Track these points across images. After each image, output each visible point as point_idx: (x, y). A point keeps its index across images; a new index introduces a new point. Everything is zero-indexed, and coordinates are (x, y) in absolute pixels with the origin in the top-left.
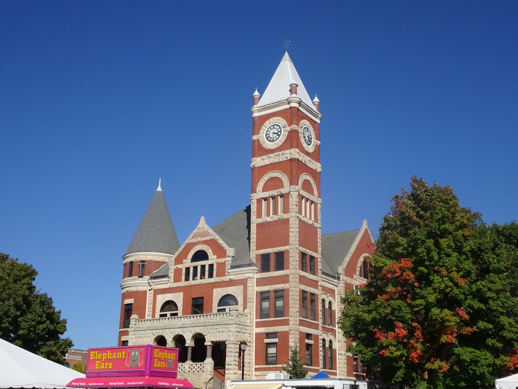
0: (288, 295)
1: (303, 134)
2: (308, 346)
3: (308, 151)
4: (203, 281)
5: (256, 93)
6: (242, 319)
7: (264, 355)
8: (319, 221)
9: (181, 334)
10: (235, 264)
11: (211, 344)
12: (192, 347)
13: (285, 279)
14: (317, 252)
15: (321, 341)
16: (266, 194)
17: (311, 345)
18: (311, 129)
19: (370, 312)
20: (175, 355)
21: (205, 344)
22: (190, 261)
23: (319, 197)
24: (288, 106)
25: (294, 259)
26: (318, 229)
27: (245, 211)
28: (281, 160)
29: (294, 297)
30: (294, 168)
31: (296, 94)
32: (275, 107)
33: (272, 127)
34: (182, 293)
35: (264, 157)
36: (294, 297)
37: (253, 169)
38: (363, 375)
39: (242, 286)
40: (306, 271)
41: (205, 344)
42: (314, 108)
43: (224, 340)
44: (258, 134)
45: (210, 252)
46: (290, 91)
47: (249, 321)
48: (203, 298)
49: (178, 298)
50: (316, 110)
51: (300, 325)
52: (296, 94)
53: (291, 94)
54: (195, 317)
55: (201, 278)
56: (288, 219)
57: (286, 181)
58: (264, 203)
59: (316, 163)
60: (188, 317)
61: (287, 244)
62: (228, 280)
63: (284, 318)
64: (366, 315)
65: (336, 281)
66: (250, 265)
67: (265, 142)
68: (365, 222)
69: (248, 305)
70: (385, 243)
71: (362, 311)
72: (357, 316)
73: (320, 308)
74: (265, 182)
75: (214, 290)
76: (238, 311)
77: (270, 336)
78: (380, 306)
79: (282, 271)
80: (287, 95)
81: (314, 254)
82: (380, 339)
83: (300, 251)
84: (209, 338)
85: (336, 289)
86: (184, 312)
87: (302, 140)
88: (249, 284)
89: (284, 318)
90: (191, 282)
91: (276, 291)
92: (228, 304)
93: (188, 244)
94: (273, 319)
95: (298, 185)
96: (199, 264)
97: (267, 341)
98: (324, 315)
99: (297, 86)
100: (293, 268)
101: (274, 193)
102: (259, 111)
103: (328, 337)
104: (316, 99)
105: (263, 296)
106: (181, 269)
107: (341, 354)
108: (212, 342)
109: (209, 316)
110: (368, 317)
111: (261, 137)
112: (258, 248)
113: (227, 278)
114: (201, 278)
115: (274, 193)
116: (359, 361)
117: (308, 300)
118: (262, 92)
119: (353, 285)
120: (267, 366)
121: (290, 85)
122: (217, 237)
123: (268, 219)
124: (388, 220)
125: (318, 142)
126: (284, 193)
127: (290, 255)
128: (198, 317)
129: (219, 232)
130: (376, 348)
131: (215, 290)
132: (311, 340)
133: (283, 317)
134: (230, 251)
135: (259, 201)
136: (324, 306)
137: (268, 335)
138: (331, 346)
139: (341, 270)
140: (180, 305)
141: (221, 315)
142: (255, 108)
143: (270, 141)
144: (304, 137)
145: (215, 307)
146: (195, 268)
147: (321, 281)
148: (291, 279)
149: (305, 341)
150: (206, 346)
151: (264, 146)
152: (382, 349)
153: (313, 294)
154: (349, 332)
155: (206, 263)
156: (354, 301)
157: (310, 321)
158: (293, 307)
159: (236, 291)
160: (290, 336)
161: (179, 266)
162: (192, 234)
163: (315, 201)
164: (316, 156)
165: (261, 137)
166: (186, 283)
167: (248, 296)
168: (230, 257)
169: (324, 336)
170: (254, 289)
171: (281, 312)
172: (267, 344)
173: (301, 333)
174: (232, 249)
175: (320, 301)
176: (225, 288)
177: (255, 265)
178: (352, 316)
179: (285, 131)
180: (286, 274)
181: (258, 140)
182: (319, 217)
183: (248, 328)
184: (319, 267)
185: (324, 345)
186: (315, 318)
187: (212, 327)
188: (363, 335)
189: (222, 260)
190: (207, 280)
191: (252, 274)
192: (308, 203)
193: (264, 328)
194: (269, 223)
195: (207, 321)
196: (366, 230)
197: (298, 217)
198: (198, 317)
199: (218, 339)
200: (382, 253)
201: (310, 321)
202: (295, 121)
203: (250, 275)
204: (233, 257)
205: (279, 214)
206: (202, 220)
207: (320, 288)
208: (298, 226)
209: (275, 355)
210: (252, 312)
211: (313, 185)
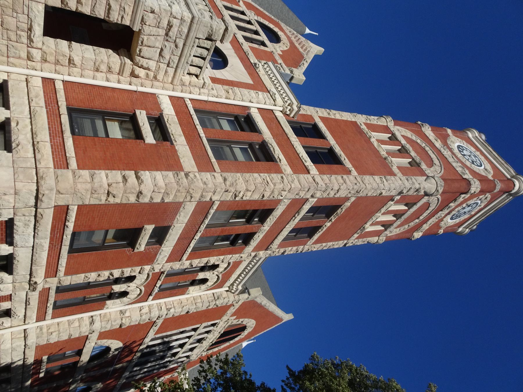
17: (132, 244)
24: (509, 177)
38: (40, 373)
62: (252, 62)
63: (213, 160)
65: (240, 288)
91: (264, 147)
94: (202, 135)
97: (142, 117)
107: (92, 322)
116: (76, 359)
120: (63, 110)
127: (345, 177)
138: (112, 296)
149: (149, 224)
160: (170, 174)
168: (292, 72)
169: (140, 279)
172: (133, 119)
183: (171, 71)
193: (173, 113)
210: (205, 91)
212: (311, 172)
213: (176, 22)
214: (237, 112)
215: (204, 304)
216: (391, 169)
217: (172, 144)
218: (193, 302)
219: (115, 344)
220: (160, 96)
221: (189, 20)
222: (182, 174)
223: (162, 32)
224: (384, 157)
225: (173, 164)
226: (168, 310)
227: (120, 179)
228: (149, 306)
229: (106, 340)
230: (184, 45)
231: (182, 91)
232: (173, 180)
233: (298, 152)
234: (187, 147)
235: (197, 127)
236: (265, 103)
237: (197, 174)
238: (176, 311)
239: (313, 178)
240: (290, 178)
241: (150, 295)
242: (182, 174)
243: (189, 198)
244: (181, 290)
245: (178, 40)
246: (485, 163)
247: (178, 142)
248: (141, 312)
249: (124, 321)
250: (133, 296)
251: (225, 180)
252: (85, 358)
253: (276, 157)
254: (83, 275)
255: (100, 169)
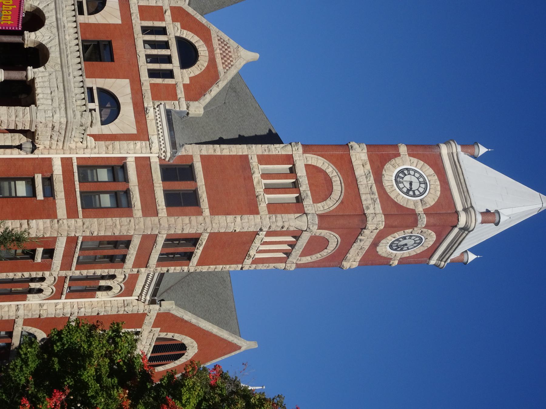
0: (121, 216)
1: (411, 236)
2: (32, 254)
3: (381, 244)
4: (142, 60)
5: (482, 150)
6: (76, 134)
7: (11, 174)
8: (254, 266)
9: (47, 22)
10: (175, 117)
11: (30, 77)
12: (23, 44)
13: (150, 210)
14: (200, 263)
15: (40, 275)
16: (301, 172)
18: (419, 250)
19: (98, 379)
20: (9, 22)
21: (29, 68)
22: (178, 34)
23: (298, 266)
24: (459, 207)
25: (185, 224)
26: (240, 266)
27: (270, 130)
28: (363, 197)
29: (118, 227)
30: (349, 220)
31: (482, 223)
32: (458, 185)
33: (421, 180)
34: (120, 22)
35: (368, 167)
36: (118, 227)
37: (347, 147)
39: (135, 132)
40: (165, 246)
41: (29, 68)
42: (456, 254)
43: (38, 103)
44: (410, 155)
45: (195, 70)
46: (488, 211)
47: (73, 145)
48: (112, 60)
49: (111, 15)
50: (452, 257)
51: (68, 238)
52: (482, 223)
53: (482, 213)
54: (77, 48)
55: (147, 56)
56: (257, 213)
57: (326, 207)
58: (285, 168)
59: (359, 258)
60: (76, 35)
61: (214, 211)
62: (146, 105)
63: (80, 209)
64: (92, 371)
65: (148, 298)
66: (174, 145)
67: (395, 167)
68: (253, 345)
69: (103, 143)
70: (222, 401)
71: (99, 365)
72: (90, 355)
73: (99, 272)
74: (324, 168)
75: (127, 81)
76: (91, 126)
77: (47, 183)
78: (110, 396)
79: (164, 203)
80: (480, 206)
81: (195, 260)
82: (51, 398)
83: (201, 234)
84: (40, 75)
85: (134, 298)
86: (85, 27)
87: (398, 235)
88: (139, 143)
89: (80, 209)
90: (140, 38)
91: (127, 192)
92: (102, 106)
93: (208, 31)
94: (78, 190)
95: (319, 228)
96: (174, 52)
97: (38, 179)
98: (87, 278)
99: (497, 224)
100: (170, 224)
101: (305, 187)
102: (451, 155)
103: (47, 286)
104: (472, 257)
105: (118, 169)
106: (162, 19)
107: (17, 310)
108: (33, 80)
109: (80, 73)
110: (88, 374)
111: (405, 160)
112: (203, 157)
113: (148, 103)
114: (147, 56)
115: (305, 187)
116: (8, 340)
117: (112, 250)
118: (483, 159)
119: (141, 327)
121: (497, 212)
122: (222, 84)
123: (257, 177)
124: (262, 405)
125: (396, 263)
126: (305, 203)
127: (193, 218)
128: (78, 54)
129: (231, 87)
130: (31, 389)
131: (127, 82)
132: (43, 258)
133: (82, 208)
134: (197, 109)
135: (289, 159)
136: (103, 278)
137: (48, 181)
138: (31, 291)
139: (168, 306)
140: (98, 19)
141: (83, 96)
142: (456, 148)
143: (397, 176)
144: (404, 238)
145: (96, 83)
146: (165, 45)
147: (147, 272)
148: (151, 220)
149: (40, 247)
150: (26, 70)
151: (388, 166)
152: (31, 402)
153: (123, 259)
154: (61, 339)
155: (175, 65)
156: (116, 347)
157: (76, 255)
158: (99, 224)
159: (126, 121)
160: (48, 221)
161: (168, 16)
162: (226, 38)
163: (291, 259)
164: (371, 258)
165: (405, 160)
166: (137, 29)
167: (117, 143)
168: (188, 108)
169: (49, 280)
170: (130, 152)
171: (90, 203)
173: (54, 239)
174: (201, 112)
175: (112, 272)
176: (131, 101)
177: (173, 155)
178: (90, 345)
179: (415, 203)
180: (160, 211)
181: (399, 155)
182: (261, 267)
183: (60, 144)
184: (173, 268)
185: (33, 280)
186: (81, 264)
187: (60, 79)
188: (57, 366)
189: (181, 94)
190: (144, 67)
191: (157, 149)
192: (286, 247)
193: (61, 172)
194: (250, 178)
195: (71, 70)
196: (240, 348)
197: (261, 230)
198: (78, 54)
199: (38, 91)
200: (204, 397)
201: (76, 255)
202: (432, 221)
203: (155, 146)
204: (188, 114)
205: (267, 196)
206: (253, 56)
207: (135, 270)
208: (245, 230)
209: (14, 195)
210: (89, 150)
211: (318, 255)
212: (159, 215)
213: (55, 125)
214: (113, 164)
215: (113, 309)
216: (258, 207)
217: (54, 199)
218: (103, 305)
219: (41, 335)
220: (54, 159)
221: (65, 123)
222: (56, 220)
223: (49, 129)
224: (257, 194)
225: (52, 214)
226: (79, 309)
227: (18, 225)
228: (64, 304)
229: (30, 328)
230: (65, 132)
231: (70, 153)
232: (49, 225)
233: (156, 197)
234: (64, 201)
235: (76, 183)
236: (141, 153)
237: (65, 221)
238: (87, 311)
239: (159, 220)
240: (137, 221)
241: (62, 294)
242: (56, 220)
243: (60, 235)
244: (89, 293)
245: (60, 131)
246: (432, 191)
247: (58, 198)
248: (57, 307)
249: (41, 312)
250: (48, 292)
251: (84, 224)
252: (16, 341)
253: (133, 203)
254: (5, 274)
255: (9, 220)
